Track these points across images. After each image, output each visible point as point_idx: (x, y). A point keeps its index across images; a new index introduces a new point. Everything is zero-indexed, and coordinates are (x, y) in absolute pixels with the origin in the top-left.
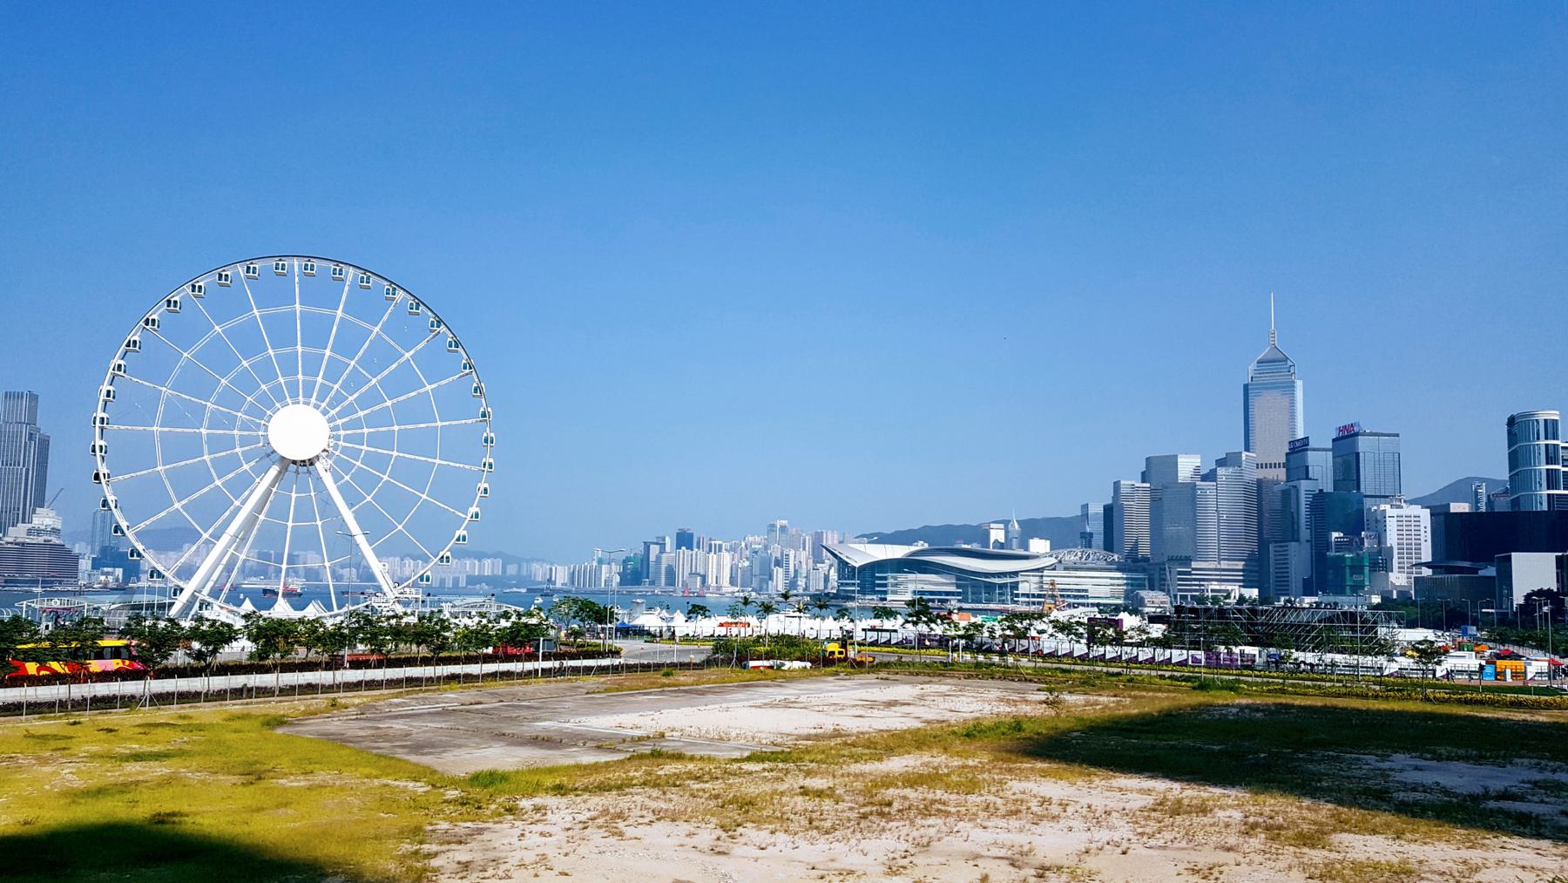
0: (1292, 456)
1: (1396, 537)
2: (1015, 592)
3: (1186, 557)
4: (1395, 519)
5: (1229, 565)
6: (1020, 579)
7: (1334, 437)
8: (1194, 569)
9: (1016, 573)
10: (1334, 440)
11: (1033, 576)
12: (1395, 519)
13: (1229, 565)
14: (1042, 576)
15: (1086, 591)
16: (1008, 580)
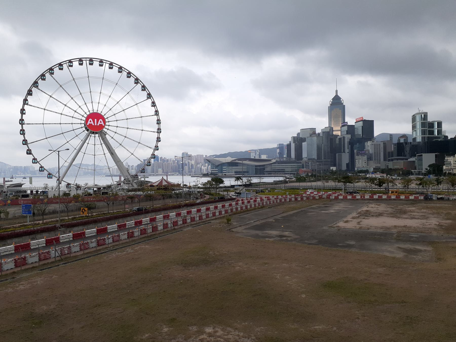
0: (342, 128)
1: (374, 150)
4: (373, 145)
6: (265, 167)
7: (355, 122)
9: (264, 165)
10: (355, 123)
11: (269, 166)
12: (373, 145)
14: (271, 166)
15: (285, 169)
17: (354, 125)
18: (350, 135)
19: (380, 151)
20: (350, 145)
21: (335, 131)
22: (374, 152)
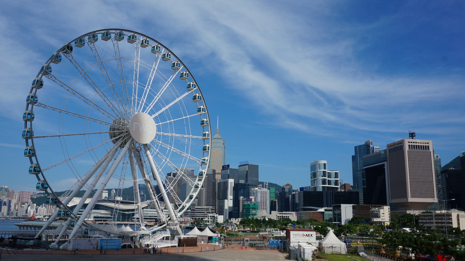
2: (133, 217)
3: (194, 204)
4: (260, 193)
5: (207, 207)
6: (135, 212)
8: (196, 209)
10: (239, 166)
13: (207, 207)
16: (131, 212)
17: (238, 170)
18: (234, 179)
19: (266, 199)
20: (234, 191)
21: (217, 174)
22: (261, 201)
